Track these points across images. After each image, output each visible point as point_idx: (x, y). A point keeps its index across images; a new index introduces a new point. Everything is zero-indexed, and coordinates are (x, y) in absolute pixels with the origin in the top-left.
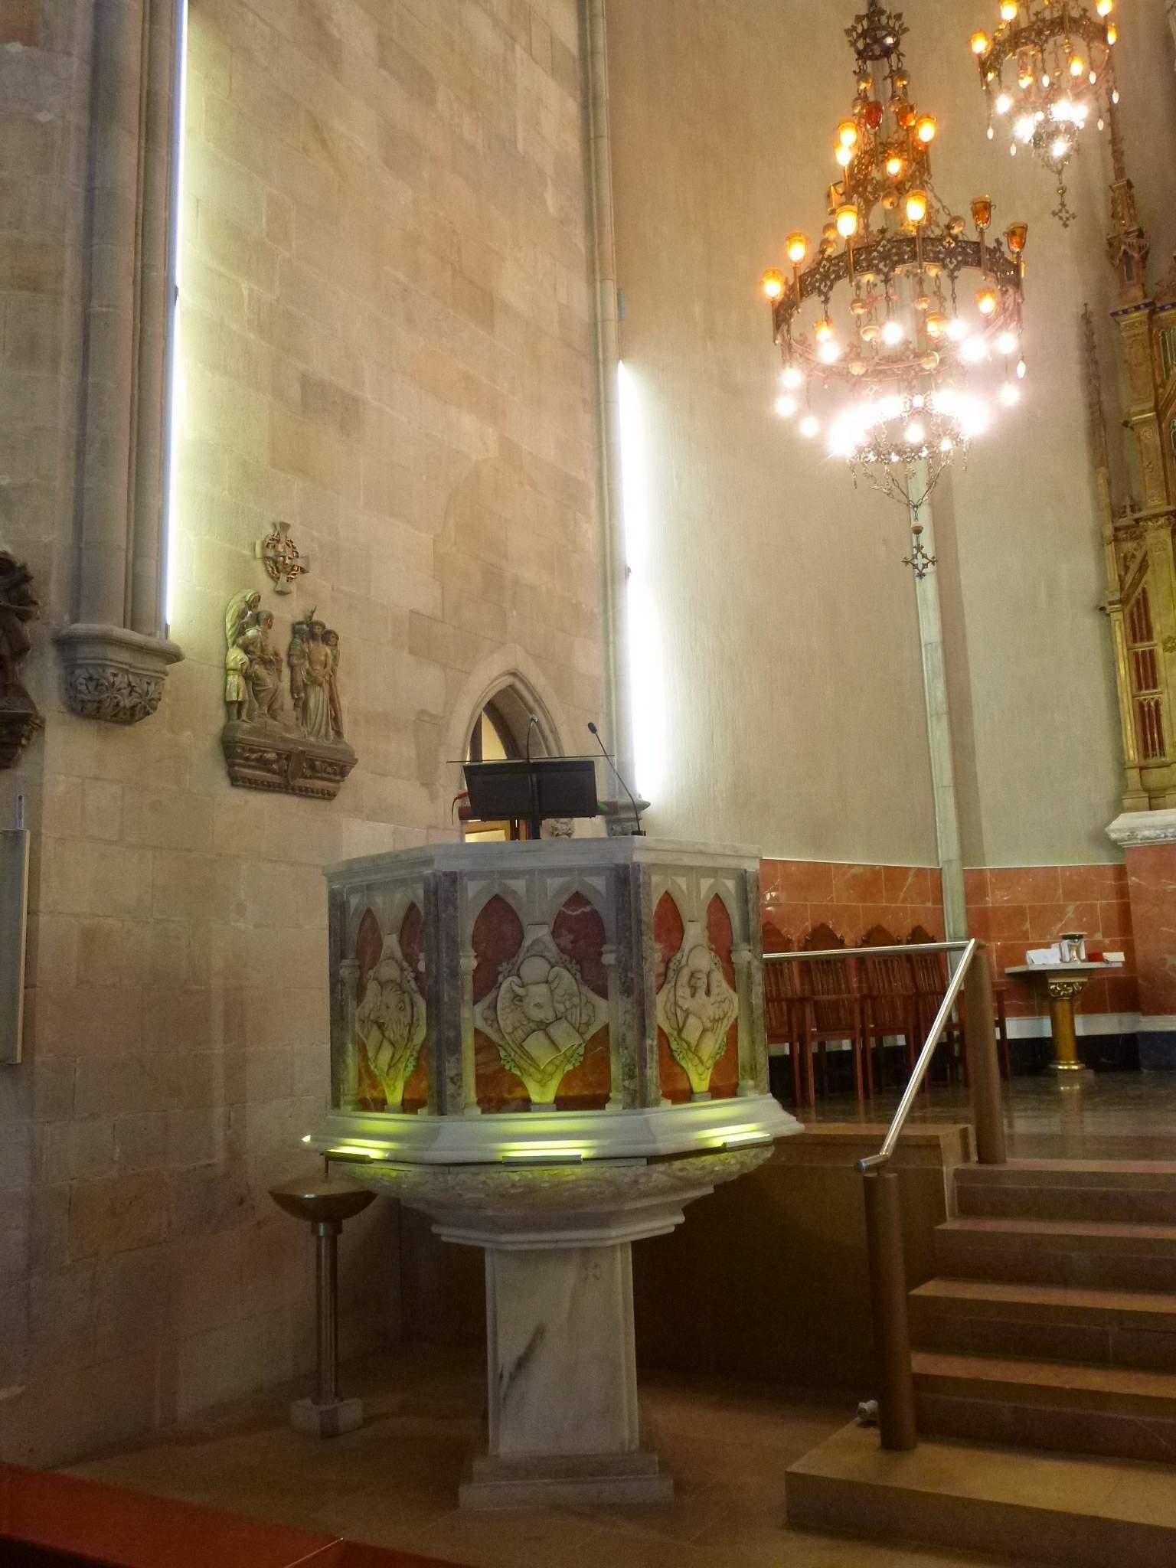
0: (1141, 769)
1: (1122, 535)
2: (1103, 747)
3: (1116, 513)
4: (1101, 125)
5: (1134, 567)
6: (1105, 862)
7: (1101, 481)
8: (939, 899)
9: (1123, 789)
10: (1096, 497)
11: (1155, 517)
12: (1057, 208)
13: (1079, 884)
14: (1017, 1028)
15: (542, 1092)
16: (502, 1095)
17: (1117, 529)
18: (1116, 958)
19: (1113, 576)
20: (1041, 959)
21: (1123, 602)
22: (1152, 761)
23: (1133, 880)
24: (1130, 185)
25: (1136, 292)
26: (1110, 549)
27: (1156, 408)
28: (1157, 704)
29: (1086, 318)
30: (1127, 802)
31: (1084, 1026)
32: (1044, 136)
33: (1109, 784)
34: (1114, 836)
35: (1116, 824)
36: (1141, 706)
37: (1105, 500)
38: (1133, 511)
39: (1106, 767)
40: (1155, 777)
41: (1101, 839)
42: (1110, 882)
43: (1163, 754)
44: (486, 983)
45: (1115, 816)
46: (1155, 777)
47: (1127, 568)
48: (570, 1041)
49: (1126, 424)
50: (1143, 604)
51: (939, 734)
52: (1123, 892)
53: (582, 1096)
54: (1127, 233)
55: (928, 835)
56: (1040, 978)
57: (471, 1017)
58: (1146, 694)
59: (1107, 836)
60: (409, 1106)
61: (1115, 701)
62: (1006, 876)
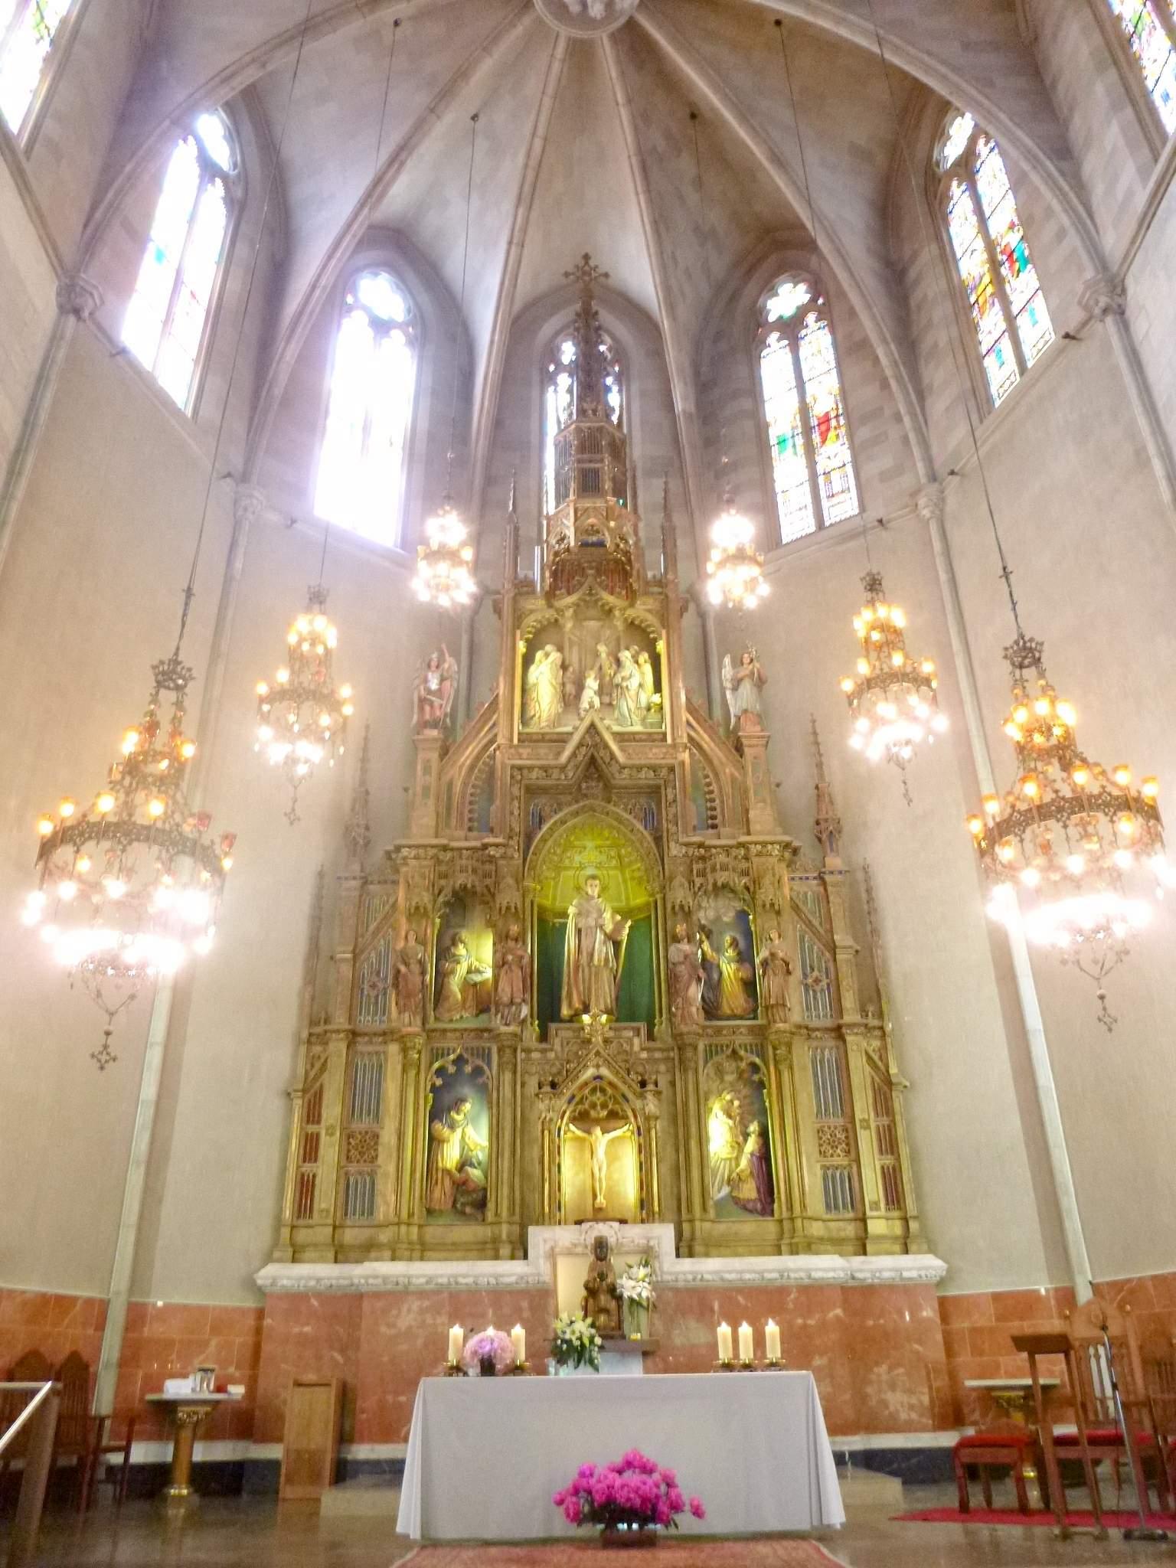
0: (293, 1227)
1: (313, 1039)
2: (268, 1204)
3: (313, 1023)
4: (332, 763)
5: (318, 1065)
6: (250, 1303)
7: (307, 996)
8: (101, 1326)
9: (276, 1243)
10: (301, 1007)
11: (338, 1031)
12: (288, 810)
14: (142, 1453)
17: (310, 1035)
18: (237, 1391)
19: (301, 1071)
20: (177, 1389)
21: (304, 1091)
22: (301, 1222)
23: (268, 1321)
24: (367, 793)
25: (356, 867)
26: (303, 1049)
27: (354, 952)
28: (314, 1176)
29: (321, 875)
30: (277, 1254)
31: (203, 1452)
32: (291, 761)
33: (265, 1238)
34: (259, 1282)
35: (263, 1272)
36: (303, 1175)
37: (307, 1010)
38: (326, 1022)
39: (266, 1223)
40: (302, 1236)
42: (251, 1322)
43: (311, 1217)
45: (265, 1264)
46: (302, 1236)
47: (313, 1066)
49: (332, 958)
50: (319, 1096)
51: (135, 1179)
52: (258, 1331)
54: (358, 826)
56: (167, 1409)
58: (307, 1168)
59: (254, 1282)
61: (283, 1170)
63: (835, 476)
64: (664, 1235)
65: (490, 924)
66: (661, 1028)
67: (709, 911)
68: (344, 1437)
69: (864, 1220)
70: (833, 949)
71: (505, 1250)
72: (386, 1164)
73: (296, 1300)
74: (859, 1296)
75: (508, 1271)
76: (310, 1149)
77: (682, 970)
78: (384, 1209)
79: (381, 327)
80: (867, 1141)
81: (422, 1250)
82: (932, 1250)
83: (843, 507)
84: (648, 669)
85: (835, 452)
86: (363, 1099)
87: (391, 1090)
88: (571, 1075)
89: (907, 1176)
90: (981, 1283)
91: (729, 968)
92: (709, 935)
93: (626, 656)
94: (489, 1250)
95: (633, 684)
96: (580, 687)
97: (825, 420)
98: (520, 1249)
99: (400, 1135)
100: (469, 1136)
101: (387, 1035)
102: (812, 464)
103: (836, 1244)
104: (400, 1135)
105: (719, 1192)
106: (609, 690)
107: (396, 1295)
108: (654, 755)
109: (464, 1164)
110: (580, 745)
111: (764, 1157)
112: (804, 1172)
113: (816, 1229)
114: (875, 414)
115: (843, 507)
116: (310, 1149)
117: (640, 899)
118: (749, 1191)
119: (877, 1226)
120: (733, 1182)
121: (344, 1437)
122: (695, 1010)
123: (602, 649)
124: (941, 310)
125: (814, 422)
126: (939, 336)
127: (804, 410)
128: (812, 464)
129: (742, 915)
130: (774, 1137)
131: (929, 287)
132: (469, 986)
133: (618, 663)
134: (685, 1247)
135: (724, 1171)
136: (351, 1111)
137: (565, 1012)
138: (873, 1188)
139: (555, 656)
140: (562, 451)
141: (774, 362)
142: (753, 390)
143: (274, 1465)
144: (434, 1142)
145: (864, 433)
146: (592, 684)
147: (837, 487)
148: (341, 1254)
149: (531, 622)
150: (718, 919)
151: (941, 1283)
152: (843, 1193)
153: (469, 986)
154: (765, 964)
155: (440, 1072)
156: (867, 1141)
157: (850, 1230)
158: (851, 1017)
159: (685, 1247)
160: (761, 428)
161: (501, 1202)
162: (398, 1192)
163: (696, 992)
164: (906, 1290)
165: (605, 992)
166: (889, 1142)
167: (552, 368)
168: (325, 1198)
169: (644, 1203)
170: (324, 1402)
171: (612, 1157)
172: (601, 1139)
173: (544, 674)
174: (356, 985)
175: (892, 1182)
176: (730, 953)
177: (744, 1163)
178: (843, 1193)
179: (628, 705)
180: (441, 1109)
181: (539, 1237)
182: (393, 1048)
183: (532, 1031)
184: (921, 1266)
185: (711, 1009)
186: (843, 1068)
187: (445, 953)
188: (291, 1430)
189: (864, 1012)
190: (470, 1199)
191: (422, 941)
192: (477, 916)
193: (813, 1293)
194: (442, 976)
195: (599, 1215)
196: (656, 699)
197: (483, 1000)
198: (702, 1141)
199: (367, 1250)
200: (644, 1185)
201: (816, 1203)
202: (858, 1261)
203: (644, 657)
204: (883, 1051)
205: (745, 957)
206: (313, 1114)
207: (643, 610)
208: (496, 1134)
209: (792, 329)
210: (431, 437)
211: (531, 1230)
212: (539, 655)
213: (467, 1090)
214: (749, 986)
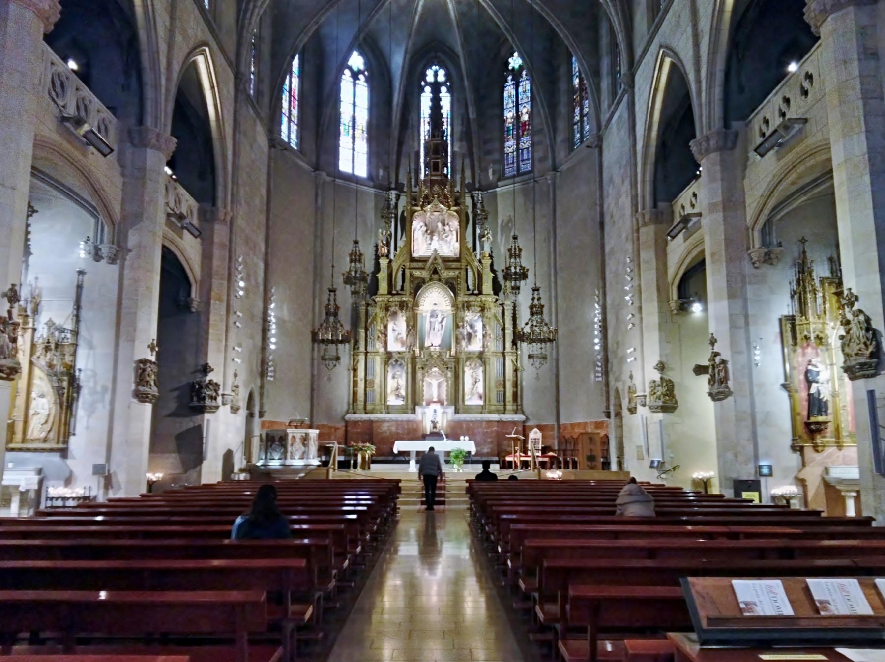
15: (297, 457)
41: (343, 418)
44: (292, 445)
63: (525, 152)
69: (505, 405)
71: (410, 411)
75: (411, 417)
79: (355, 75)
82: (523, 413)
83: (526, 167)
85: (526, 142)
89: (519, 393)
97: (524, 124)
98: (414, 411)
103: (498, 412)
114: (541, 131)
119: (510, 407)
124: (563, 99)
127: (518, 117)
128: (518, 144)
131: (563, 86)
134: (457, 412)
141: (509, 90)
147: (525, 157)
151: (524, 422)
157: (502, 408)
167: (423, 83)
189: (512, 349)
193: (489, 422)
202: (502, 416)
209: (516, 75)
211: (417, 407)
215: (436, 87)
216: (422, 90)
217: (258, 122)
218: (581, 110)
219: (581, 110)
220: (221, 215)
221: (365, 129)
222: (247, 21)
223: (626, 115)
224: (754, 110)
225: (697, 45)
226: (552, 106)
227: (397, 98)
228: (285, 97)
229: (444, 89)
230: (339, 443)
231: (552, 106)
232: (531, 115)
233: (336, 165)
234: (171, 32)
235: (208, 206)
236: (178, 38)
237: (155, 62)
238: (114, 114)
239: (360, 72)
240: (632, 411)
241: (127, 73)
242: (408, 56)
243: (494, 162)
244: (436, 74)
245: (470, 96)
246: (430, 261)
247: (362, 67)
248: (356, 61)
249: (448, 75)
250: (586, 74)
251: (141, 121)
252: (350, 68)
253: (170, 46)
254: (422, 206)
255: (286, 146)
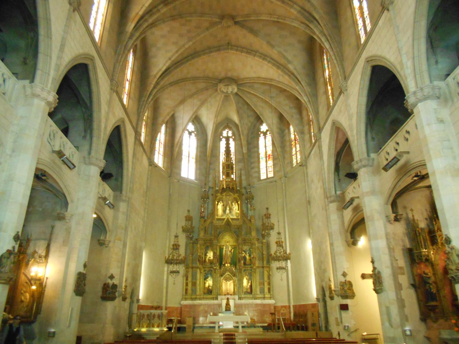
6: (180, 306)
9: (183, 298)
13: (177, 309)
16: (153, 326)
40: (187, 297)
41: (180, 304)
48: (158, 323)
52: (181, 310)
53: (158, 327)
55: (162, 302)
57: (152, 321)
60: (147, 327)
61: (183, 287)
62: (169, 307)
63: (270, 168)
64: (237, 297)
65: (212, 250)
66: (238, 267)
67: (245, 248)
68: (194, 324)
70: (263, 254)
72: (198, 287)
73: (186, 306)
74: (264, 305)
75: (215, 302)
76: (187, 284)
77: (241, 258)
78: (198, 293)
79: (190, 133)
80: (266, 284)
81: (204, 298)
82: (274, 299)
83: (271, 175)
84: (237, 206)
85: (270, 163)
86: (194, 277)
87: (198, 276)
88: (224, 274)
90: (279, 304)
91: (247, 257)
92: (245, 252)
93: (233, 204)
94: (213, 299)
95: (235, 209)
96: (226, 209)
97: (269, 156)
98: (217, 298)
99: (200, 282)
100: (209, 282)
101: (198, 268)
102: (267, 164)
104: (200, 282)
105: (245, 290)
106: (231, 209)
107: (200, 305)
108: (237, 223)
109: (209, 286)
110: (226, 221)
111: (251, 286)
112: (256, 289)
113: (258, 296)
115: (271, 175)
116: (187, 284)
117: (235, 244)
118: (249, 290)
119: (267, 296)
120: (247, 289)
121: (194, 324)
122: (242, 265)
123: (230, 202)
124: (288, 144)
125: (267, 156)
126: (288, 149)
129: (250, 249)
130: (253, 283)
132: (209, 260)
133: (232, 205)
134: (240, 298)
135: (246, 287)
136: (192, 279)
137: (223, 263)
138: (266, 290)
139: (222, 204)
140: (223, 168)
142: (257, 146)
143: (185, 328)
144: (205, 283)
145: (275, 162)
146: (228, 208)
148: (192, 299)
149: (218, 198)
150: (246, 249)
151: (275, 304)
152: (262, 291)
153: (209, 260)
154: (253, 258)
155: (205, 273)
156: (266, 284)
158: (265, 265)
159: (240, 298)
160: (259, 154)
161: (214, 292)
162: (200, 291)
163: (242, 262)
164: (269, 305)
165: (229, 260)
166: (269, 284)
167: (221, 137)
168: (189, 291)
169: (234, 292)
170: (191, 319)
171: (230, 285)
172: (229, 283)
173: (220, 207)
174: (193, 260)
175: (269, 289)
176: (248, 255)
177: (248, 286)
178: (262, 291)
179: (234, 213)
180: (206, 279)
181: (219, 297)
182: (198, 270)
183: (218, 268)
184: (272, 302)
185: (245, 264)
186: (263, 272)
187: (206, 255)
188: (187, 323)
189: (267, 264)
190: (209, 291)
191: (202, 254)
192: (210, 248)
194: (205, 258)
195: (228, 294)
196: (238, 212)
197: (211, 262)
198: (242, 283)
199: (195, 299)
200: (234, 290)
201: (258, 292)
202: (263, 301)
203: (236, 204)
204: (269, 270)
205: (250, 256)
206: (187, 279)
207: (236, 196)
208: (213, 282)
209: (265, 134)
210: (200, 156)
212: (219, 203)
213: (209, 276)
214: (250, 260)
215: (227, 139)
216: (221, 140)
217: (144, 154)
218: (296, 149)
219: (296, 149)
220: (124, 198)
221: (194, 158)
222: (142, 110)
223: (318, 151)
224: (381, 149)
225: (350, 118)
226: (283, 147)
227: (209, 144)
228: (157, 143)
229: (231, 140)
230: (178, 317)
231: (283, 147)
232: (273, 151)
233: (180, 174)
234: (108, 113)
235: (118, 193)
236: (111, 116)
237: (99, 126)
238: (78, 150)
239: (192, 132)
240: (332, 298)
241: (85, 131)
242: (215, 125)
243: (256, 172)
244: (227, 134)
245: (244, 143)
246: (225, 220)
247: (193, 130)
248: (191, 127)
249: (233, 134)
250: (297, 133)
251: (89, 153)
252: (188, 130)
253: (107, 120)
254: (221, 193)
255: (156, 166)
